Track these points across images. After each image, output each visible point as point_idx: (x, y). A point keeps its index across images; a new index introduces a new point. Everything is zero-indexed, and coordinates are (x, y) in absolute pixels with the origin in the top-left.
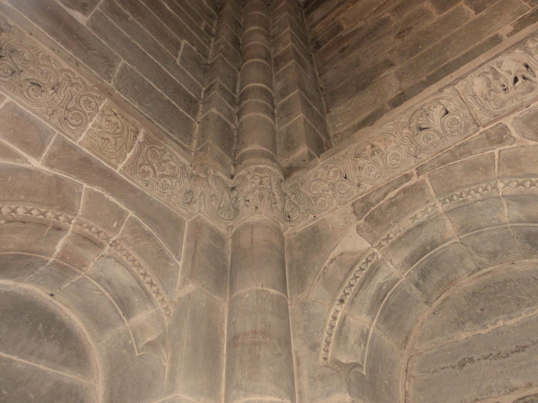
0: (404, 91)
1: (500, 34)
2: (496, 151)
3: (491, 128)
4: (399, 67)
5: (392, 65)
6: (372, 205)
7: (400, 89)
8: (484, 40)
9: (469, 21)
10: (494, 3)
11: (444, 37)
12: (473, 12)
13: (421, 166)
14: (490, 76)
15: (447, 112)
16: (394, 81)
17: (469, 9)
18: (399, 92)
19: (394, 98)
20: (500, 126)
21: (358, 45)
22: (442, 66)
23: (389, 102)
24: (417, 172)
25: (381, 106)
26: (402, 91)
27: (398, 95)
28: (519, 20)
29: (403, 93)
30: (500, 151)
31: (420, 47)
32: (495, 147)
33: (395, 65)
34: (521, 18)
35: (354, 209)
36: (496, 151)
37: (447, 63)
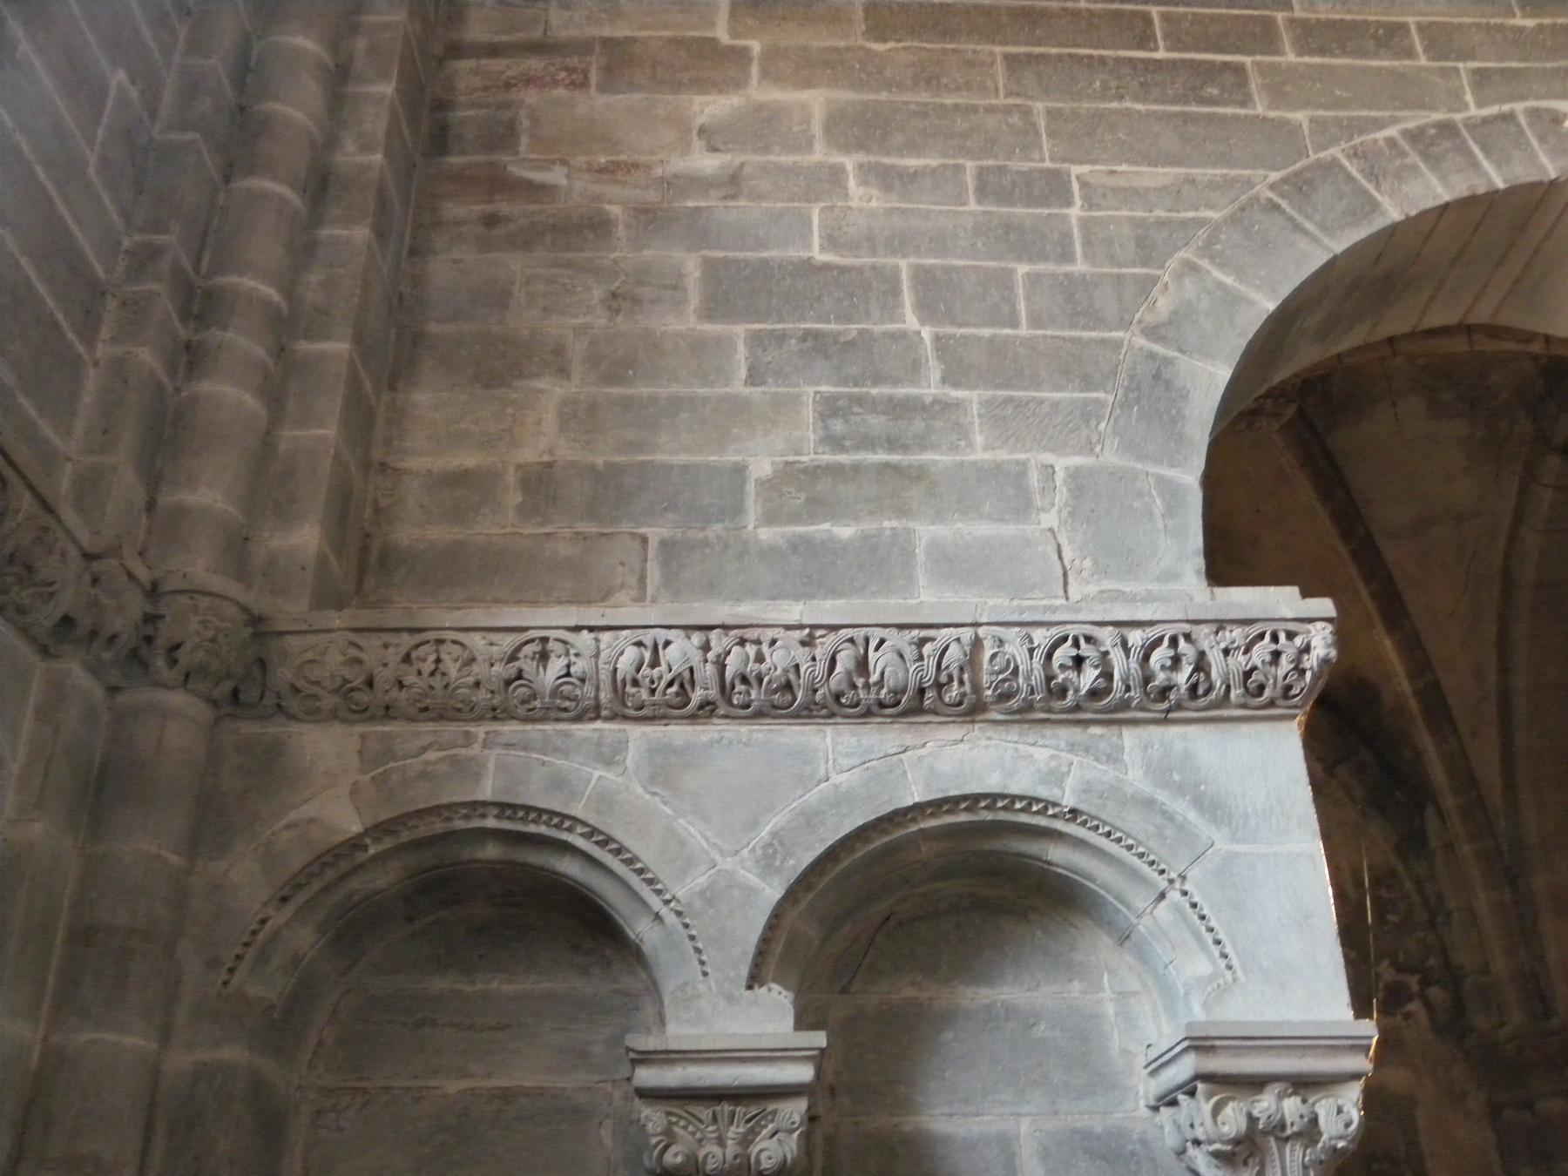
0: (556, 461)
1: (750, 468)
2: (596, 774)
3: (610, 730)
4: (574, 390)
5: (563, 372)
6: (395, 759)
7: (551, 452)
8: (725, 458)
9: (729, 390)
10: (779, 386)
11: (677, 389)
12: (743, 373)
13: (494, 731)
14: (647, 655)
15: (568, 674)
16: (550, 420)
17: (743, 358)
18: (546, 458)
19: (533, 464)
20: (621, 735)
21: (526, 239)
22: (641, 458)
23: (519, 467)
24: (485, 740)
25: (500, 465)
26: (551, 459)
27: (542, 463)
28: (787, 463)
29: (550, 465)
30: (600, 776)
31: (631, 372)
32: (599, 766)
33: (569, 377)
34: (792, 463)
35: (362, 746)
36: (596, 774)
37: (650, 458)
